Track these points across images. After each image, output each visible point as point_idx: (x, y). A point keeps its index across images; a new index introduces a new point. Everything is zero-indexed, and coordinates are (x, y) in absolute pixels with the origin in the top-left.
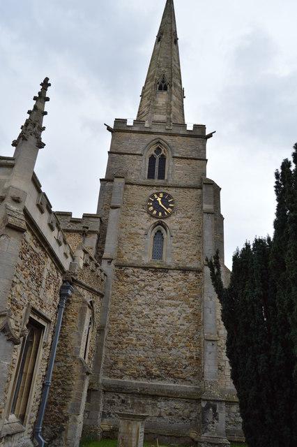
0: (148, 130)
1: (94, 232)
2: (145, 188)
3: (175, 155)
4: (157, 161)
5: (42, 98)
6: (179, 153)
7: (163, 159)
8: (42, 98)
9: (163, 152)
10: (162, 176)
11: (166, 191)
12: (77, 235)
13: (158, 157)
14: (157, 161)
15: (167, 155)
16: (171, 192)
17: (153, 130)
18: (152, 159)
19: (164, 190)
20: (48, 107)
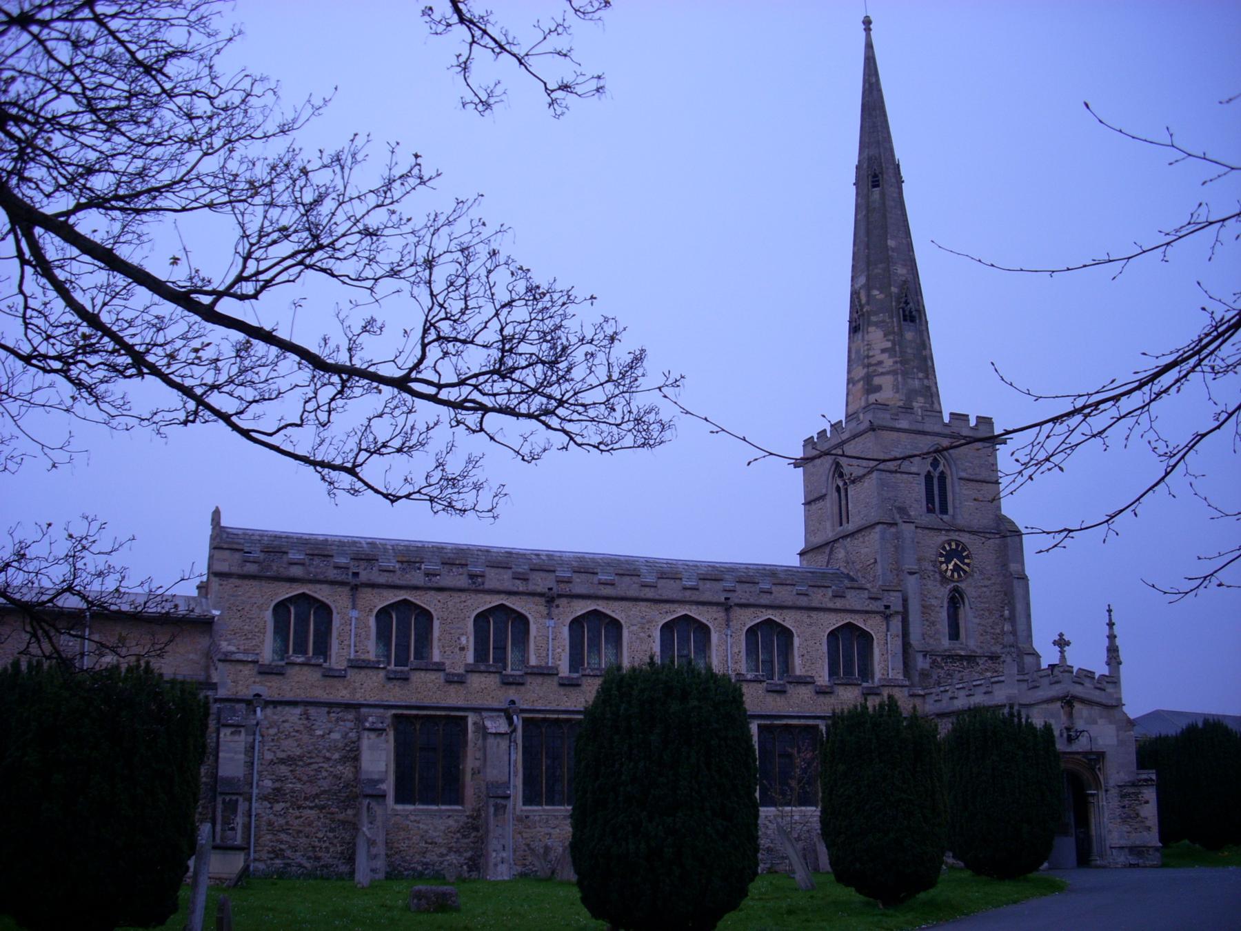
0: (920, 427)
1: (897, 613)
2: (932, 533)
3: (963, 475)
4: (936, 481)
5: (1112, 637)
6: (965, 470)
7: (942, 477)
8: (1112, 637)
9: (941, 468)
10: (944, 510)
11: (958, 538)
12: (878, 617)
13: (936, 474)
14: (936, 481)
15: (948, 473)
16: (965, 538)
17: (929, 426)
18: (929, 478)
19: (955, 536)
20: (1118, 642)
